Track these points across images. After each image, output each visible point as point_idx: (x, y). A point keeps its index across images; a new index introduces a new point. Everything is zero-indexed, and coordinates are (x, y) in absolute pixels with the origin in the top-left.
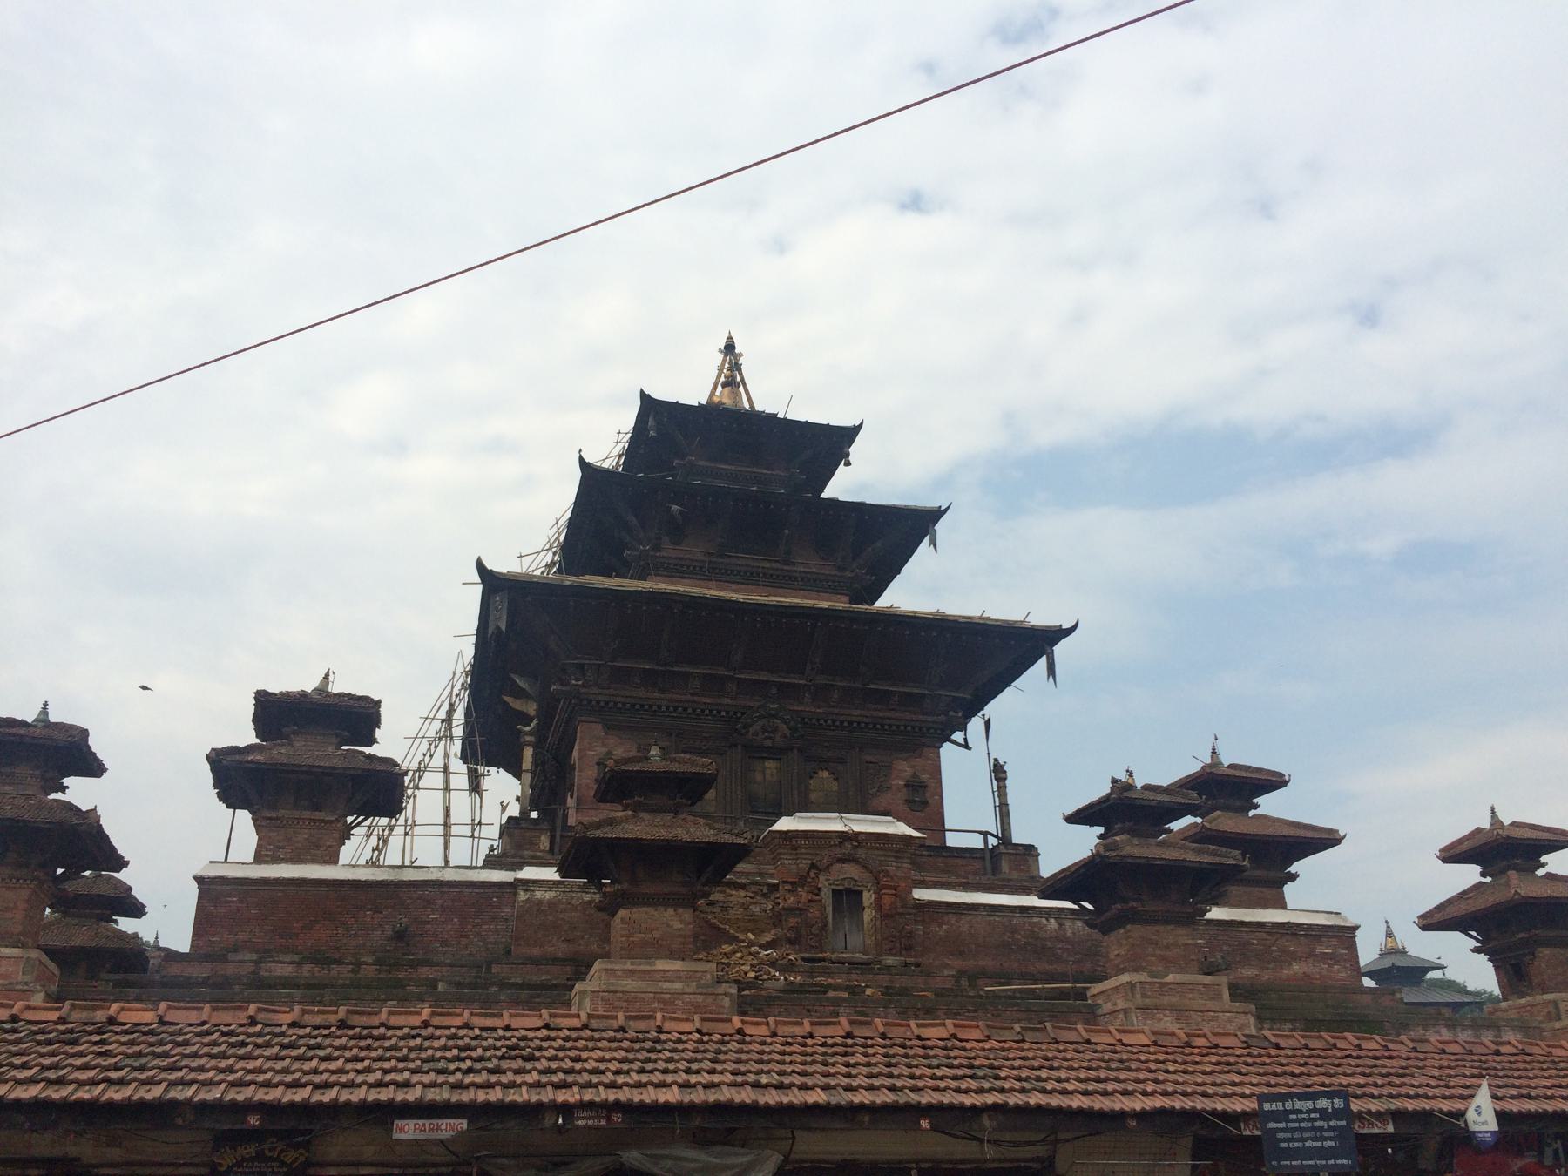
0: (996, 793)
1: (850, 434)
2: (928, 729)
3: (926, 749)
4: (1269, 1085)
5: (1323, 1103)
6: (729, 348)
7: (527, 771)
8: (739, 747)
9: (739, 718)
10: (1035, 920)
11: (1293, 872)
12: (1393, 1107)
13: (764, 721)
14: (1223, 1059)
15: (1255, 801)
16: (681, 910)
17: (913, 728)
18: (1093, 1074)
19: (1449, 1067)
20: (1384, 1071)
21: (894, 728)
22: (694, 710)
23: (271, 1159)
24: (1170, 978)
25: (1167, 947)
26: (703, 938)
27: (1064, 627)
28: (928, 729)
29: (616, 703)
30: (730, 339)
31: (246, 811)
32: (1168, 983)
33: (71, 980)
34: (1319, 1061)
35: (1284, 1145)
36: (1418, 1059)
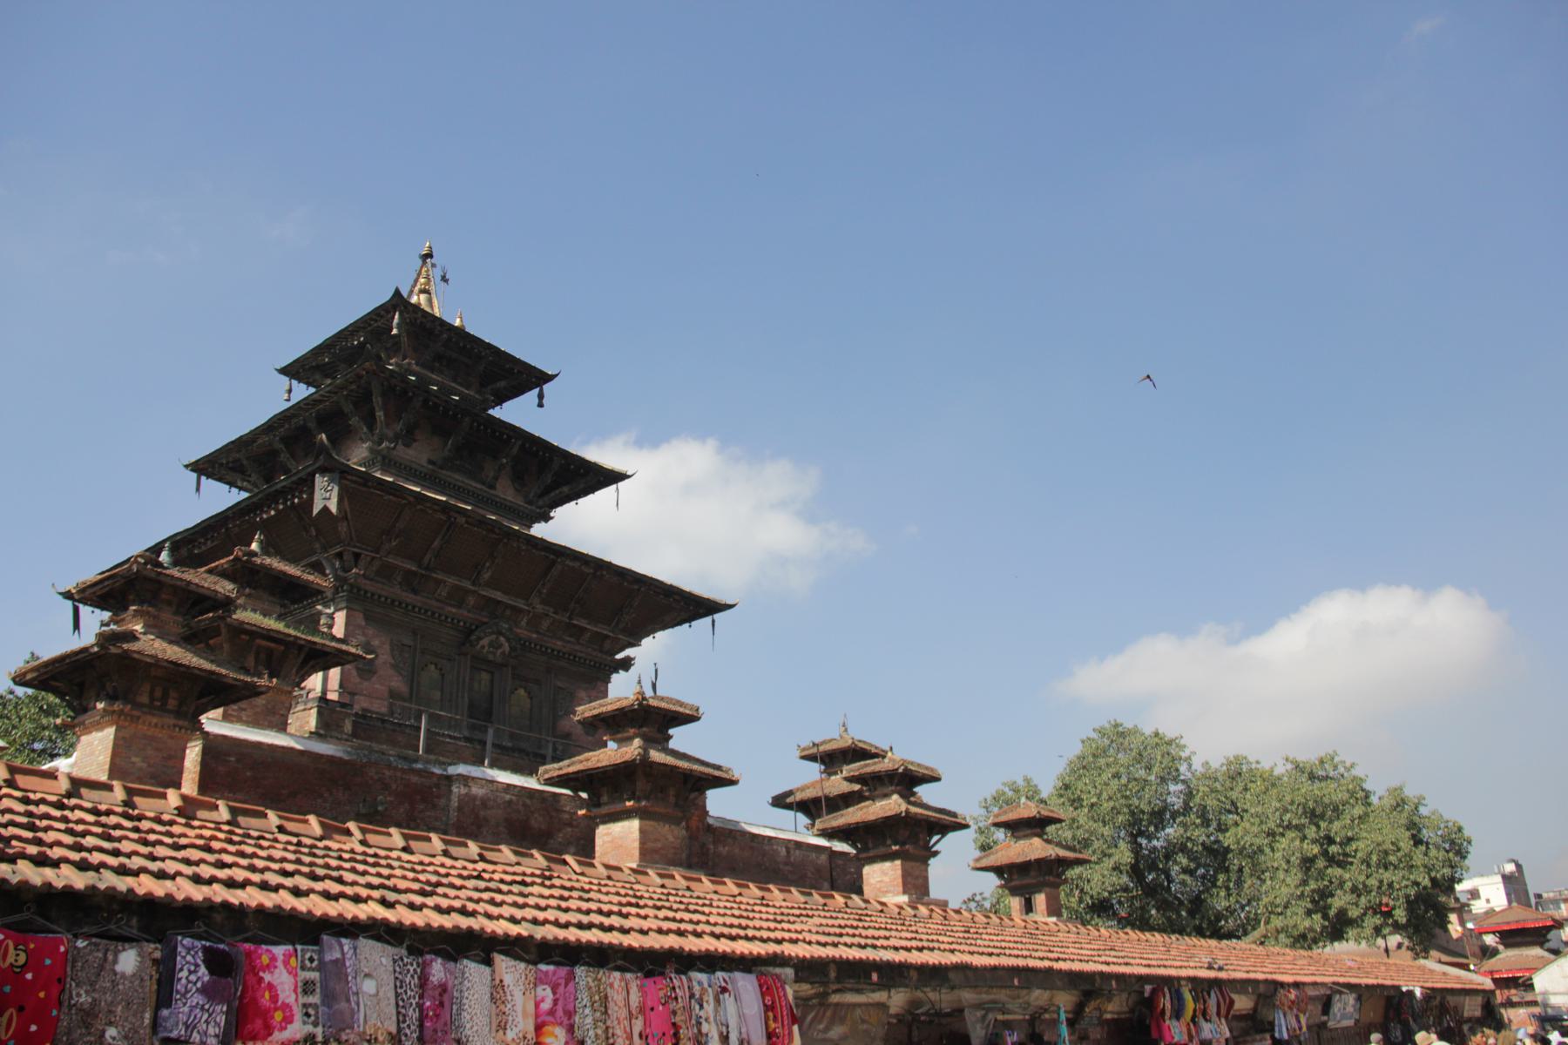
1: (550, 378)
2: (606, 666)
3: (599, 683)
8: (469, 657)
9: (471, 632)
10: (775, 847)
13: (494, 637)
16: (673, 827)
17: (595, 663)
21: (582, 661)
22: (440, 615)
25: (917, 878)
26: (582, 842)
28: (606, 666)
29: (380, 596)
33: (1106, 894)
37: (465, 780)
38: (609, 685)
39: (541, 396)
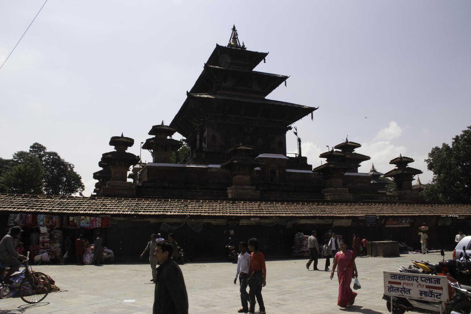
0: (298, 145)
1: (266, 54)
4: (362, 212)
5: (373, 216)
6: (234, 29)
7: (198, 140)
11: (360, 165)
12: (379, 215)
14: (356, 208)
15: (354, 150)
16: (248, 176)
18: (338, 211)
19: (387, 209)
20: (378, 209)
23: (235, 223)
24: (338, 189)
27: (316, 108)
30: (234, 26)
31: (147, 150)
32: (337, 190)
34: (369, 208)
35: (368, 221)
36: (383, 207)
37: (210, 168)
38: (286, 134)
39: (265, 60)
